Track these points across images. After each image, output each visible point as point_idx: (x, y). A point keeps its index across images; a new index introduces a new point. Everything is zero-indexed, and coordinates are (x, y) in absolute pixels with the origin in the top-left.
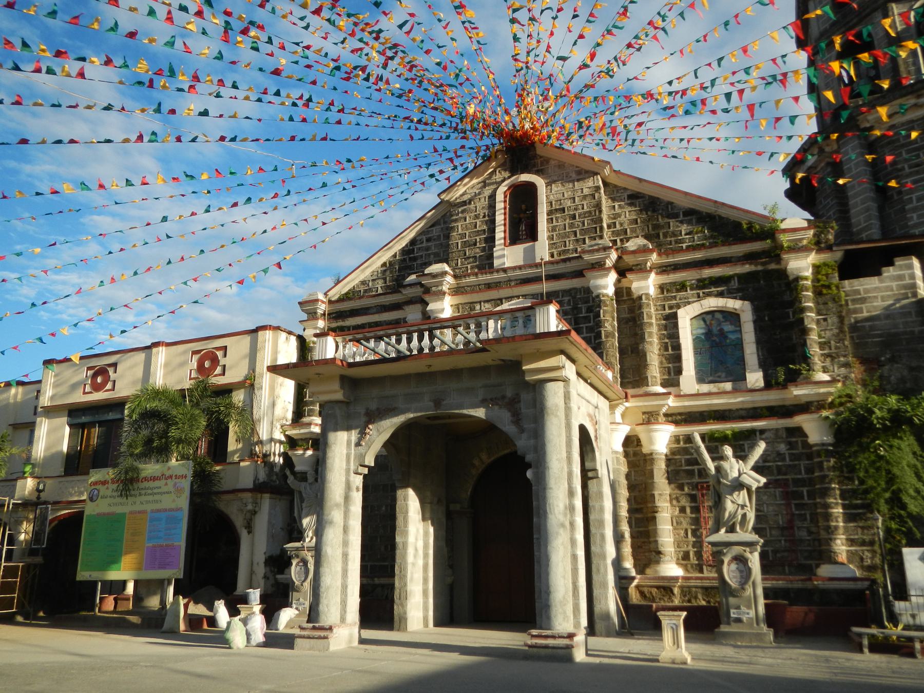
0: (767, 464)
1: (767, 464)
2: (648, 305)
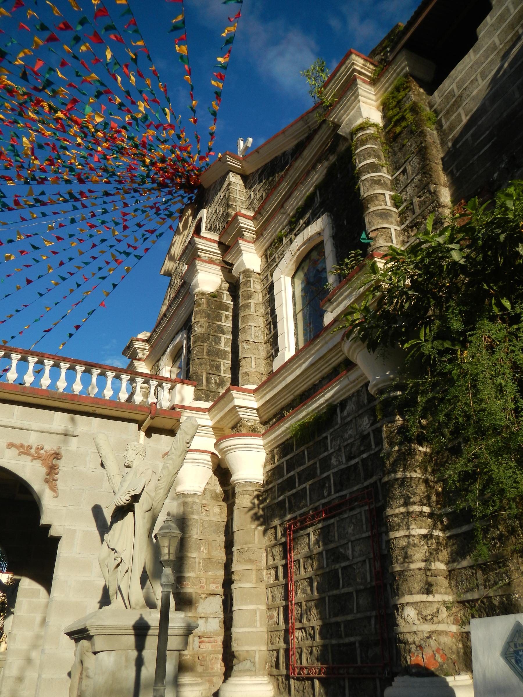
0: (353, 462)
1: (353, 462)
2: (247, 283)
